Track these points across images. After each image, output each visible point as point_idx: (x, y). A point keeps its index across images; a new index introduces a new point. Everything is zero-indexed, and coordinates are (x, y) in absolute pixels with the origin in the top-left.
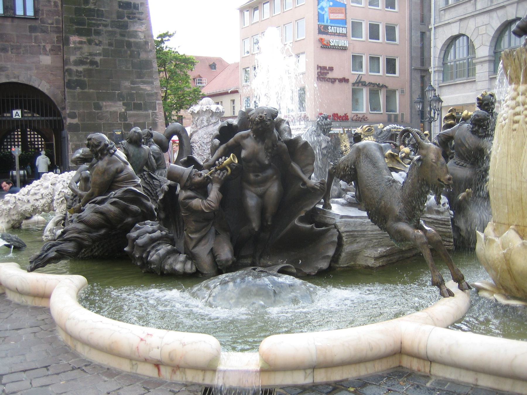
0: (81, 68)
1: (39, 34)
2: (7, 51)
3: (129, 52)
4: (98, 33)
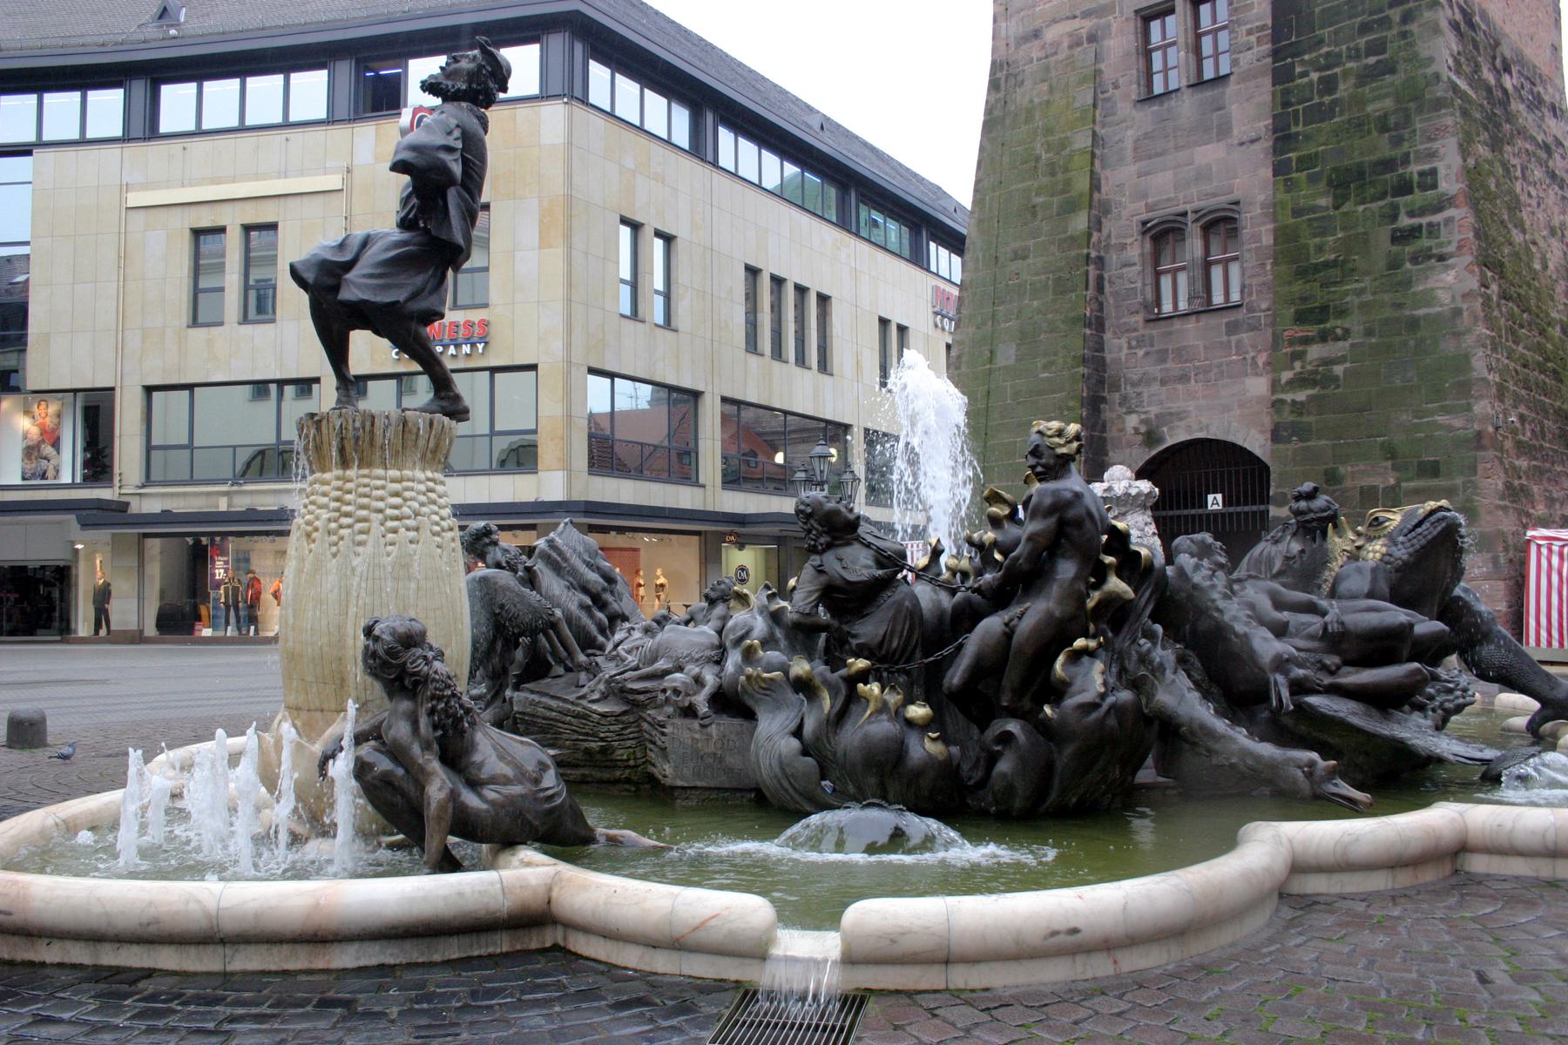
0: (1301, 396)
1: (1244, 335)
2: (1188, 380)
3: (1412, 343)
4: (1342, 313)
